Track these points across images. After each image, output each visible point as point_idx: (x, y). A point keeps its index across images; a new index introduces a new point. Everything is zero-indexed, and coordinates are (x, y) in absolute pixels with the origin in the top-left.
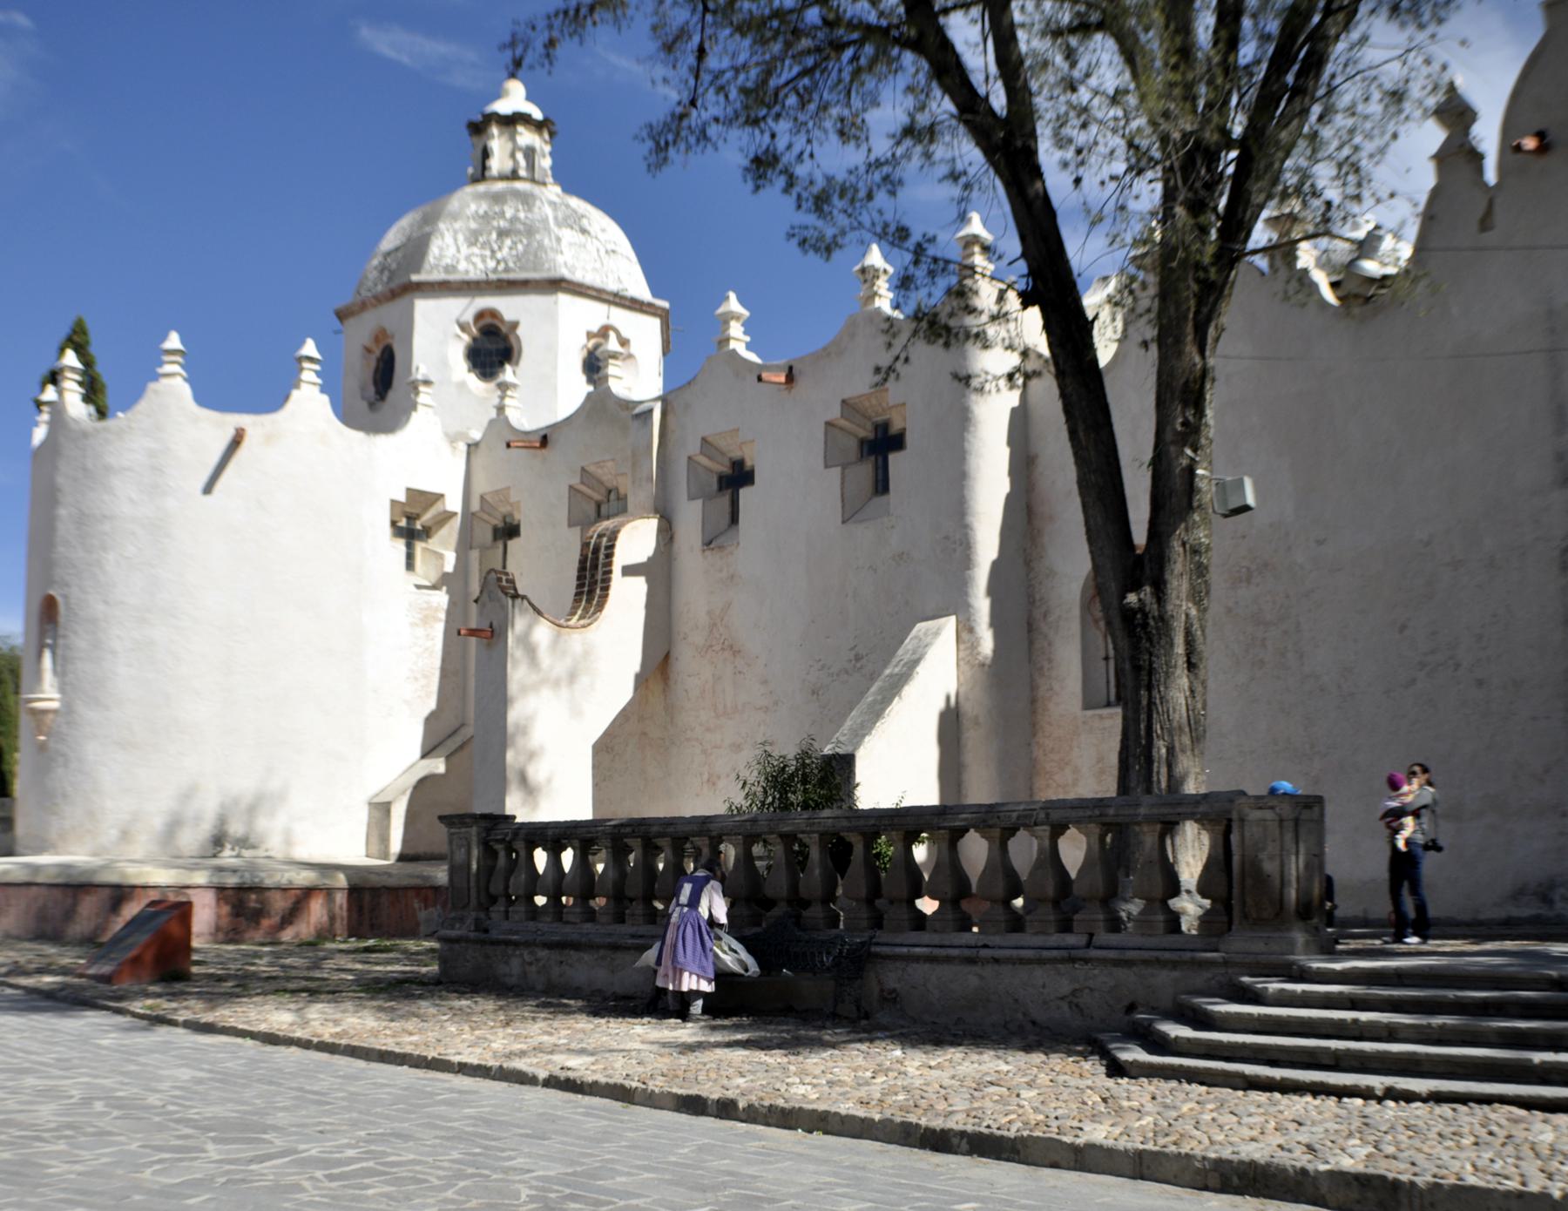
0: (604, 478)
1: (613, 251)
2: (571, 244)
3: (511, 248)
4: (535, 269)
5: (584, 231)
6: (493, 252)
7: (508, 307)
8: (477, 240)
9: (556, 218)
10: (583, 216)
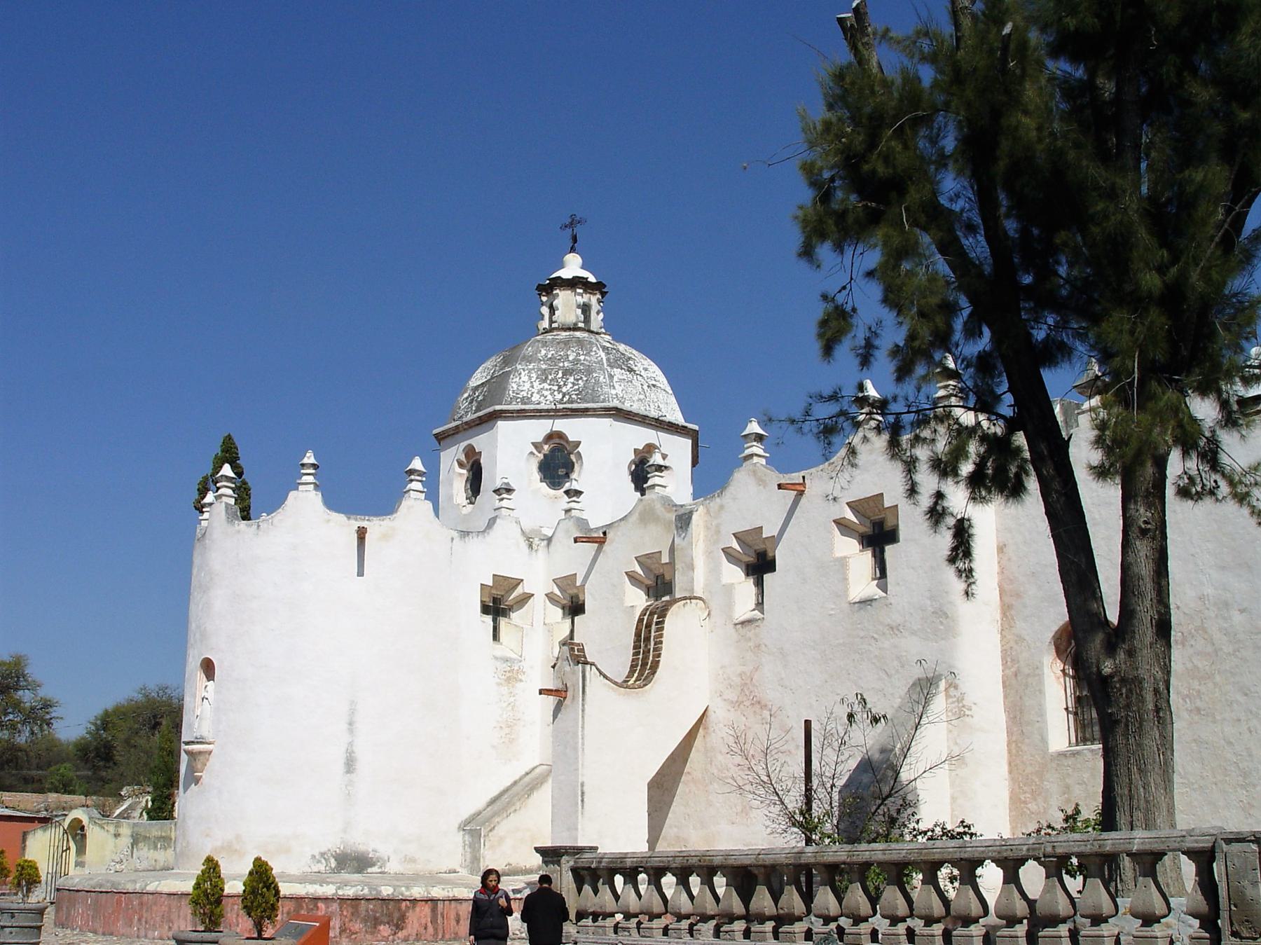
0: (653, 567)
1: (654, 386)
2: (621, 380)
3: (573, 383)
4: (594, 402)
5: (631, 370)
6: (560, 387)
7: (571, 428)
8: (547, 378)
9: (608, 360)
10: (630, 358)
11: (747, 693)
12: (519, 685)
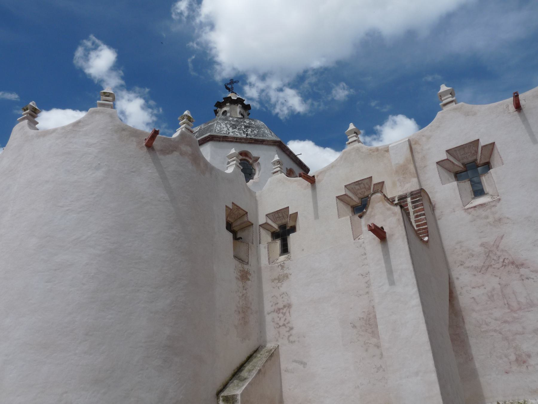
3: (252, 132)
6: (244, 132)
7: (255, 151)
11: (495, 258)
12: (249, 283)
